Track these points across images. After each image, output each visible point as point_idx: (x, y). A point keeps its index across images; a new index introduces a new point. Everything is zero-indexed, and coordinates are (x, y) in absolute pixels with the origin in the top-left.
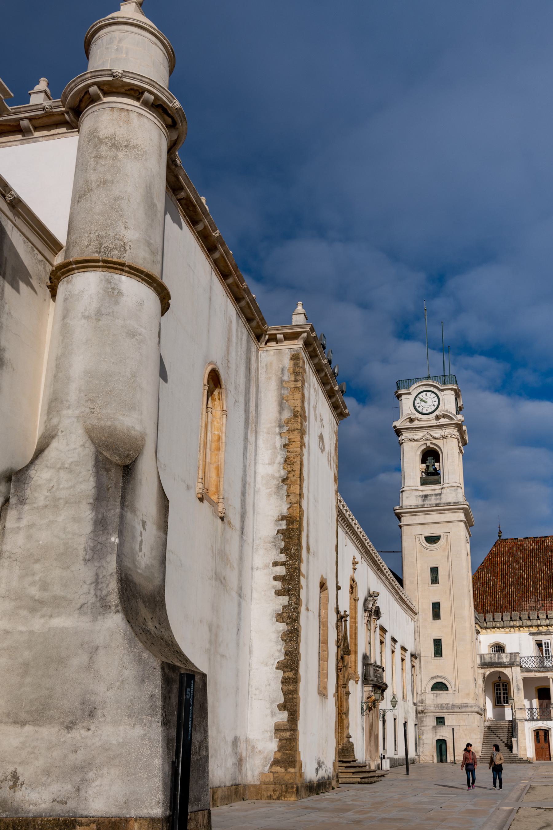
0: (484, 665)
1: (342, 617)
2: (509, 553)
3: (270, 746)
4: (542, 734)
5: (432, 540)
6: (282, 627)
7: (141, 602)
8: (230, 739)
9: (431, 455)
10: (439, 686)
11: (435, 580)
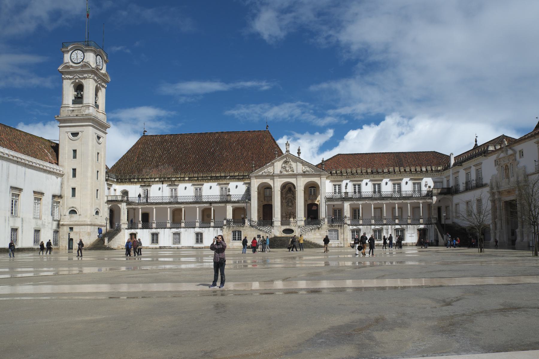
0: (108, 202)
5: (75, 134)
9: (79, 88)
11: (75, 157)
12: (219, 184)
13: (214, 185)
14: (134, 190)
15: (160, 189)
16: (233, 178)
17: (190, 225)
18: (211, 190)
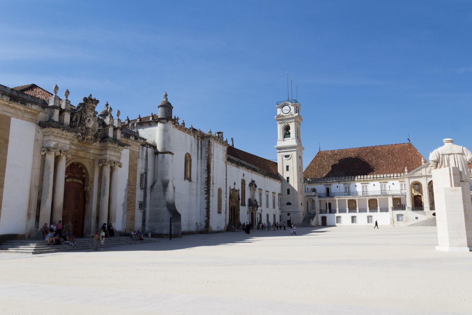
1: (237, 191)
2: (322, 157)
3: (205, 224)
4: (324, 218)
5: (287, 156)
6: (206, 201)
8: (195, 222)
9: (287, 128)
10: (289, 204)
12: (380, 183)
13: (377, 183)
15: (337, 187)
17: (362, 210)
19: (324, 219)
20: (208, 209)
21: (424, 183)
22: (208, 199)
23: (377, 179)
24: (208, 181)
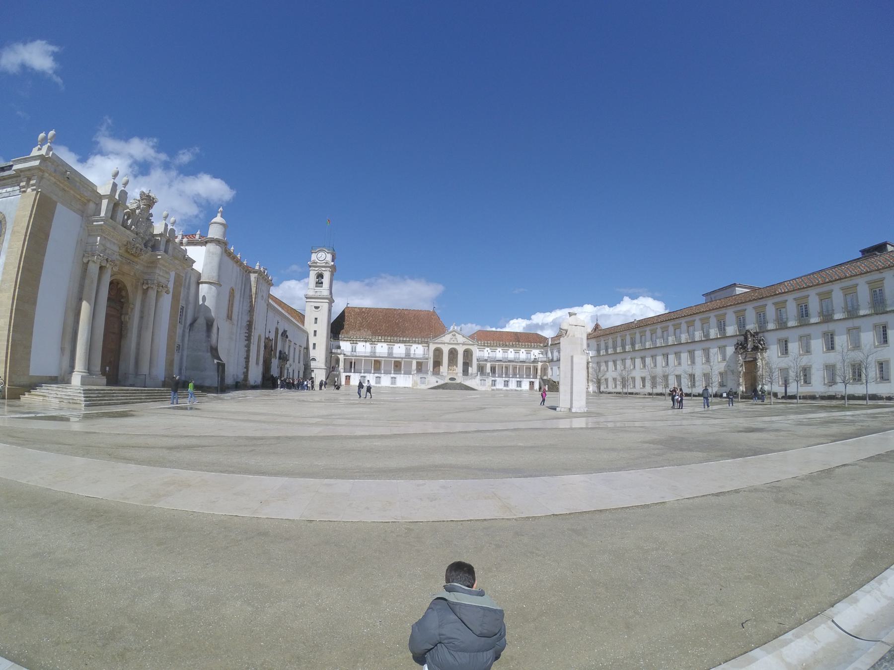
7: (214, 351)
9: (320, 276)
11: (316, 323)
13: (402, 346)
14: (346, 346)
16: (415, 342)
17: (387, 372)
18: (399, 350)
19: (348, 378)
20: (247, 358)
21: (446, 350)
22: (248, 347)
23: (403, 342)
24: (250, 326)
